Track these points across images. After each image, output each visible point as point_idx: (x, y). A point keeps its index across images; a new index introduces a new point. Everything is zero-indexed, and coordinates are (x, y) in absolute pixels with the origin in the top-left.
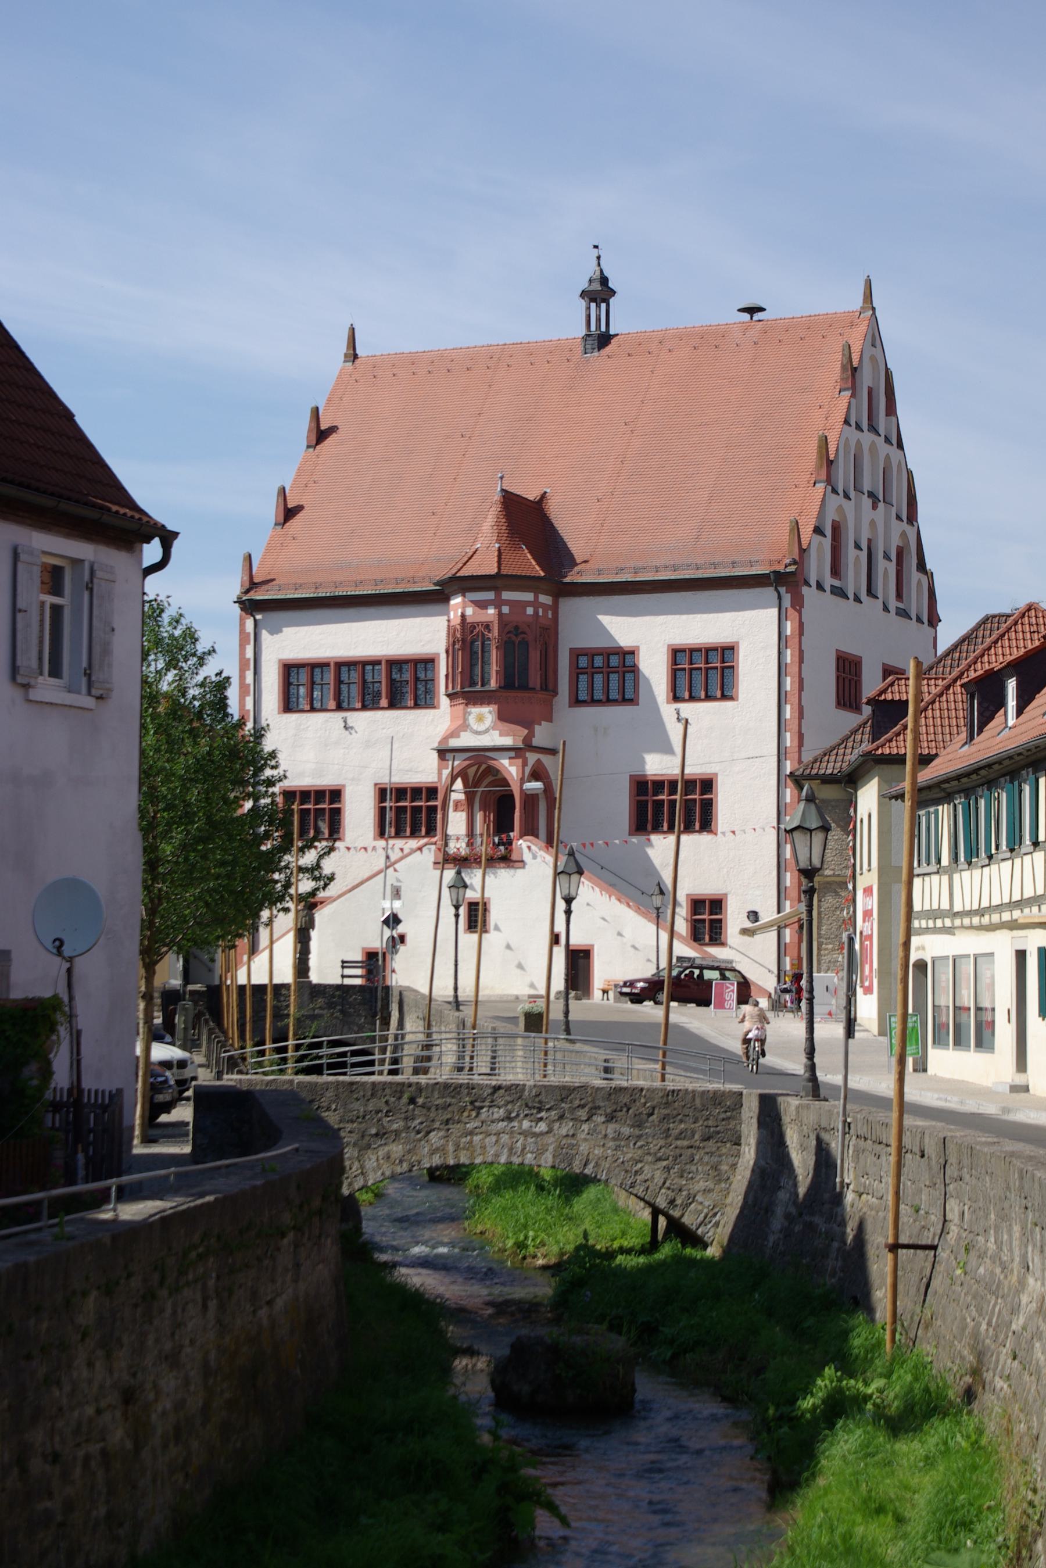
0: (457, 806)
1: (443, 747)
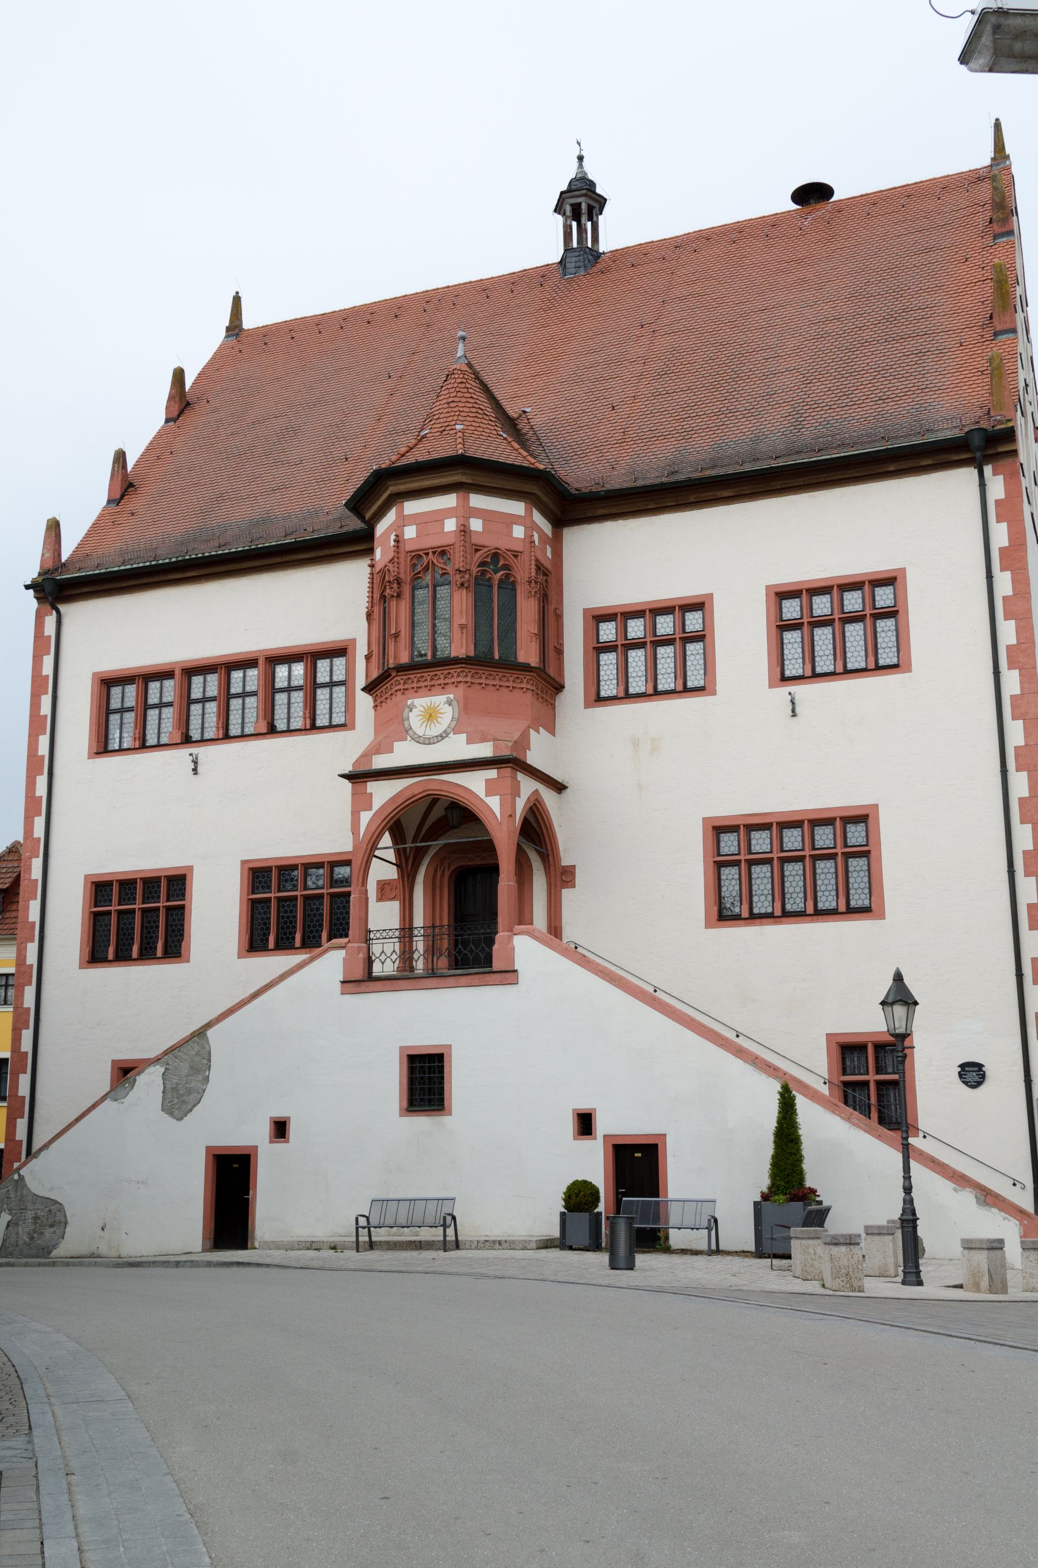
0: (385, 890)
1: (363, 768)
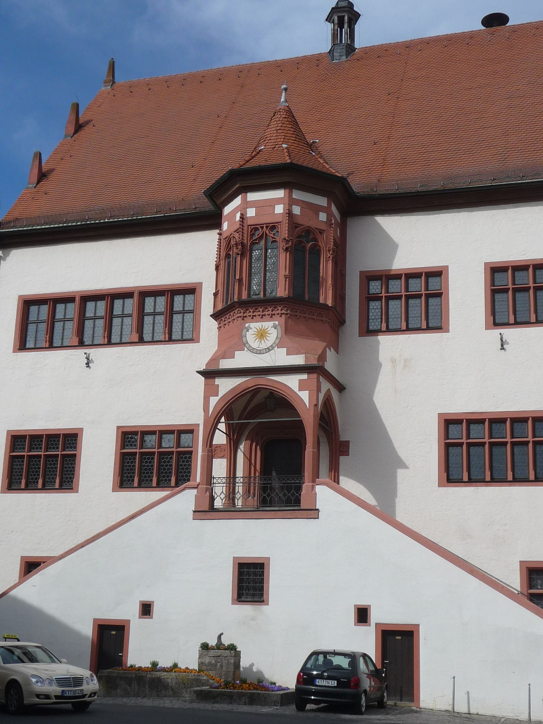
1: (213, 368)
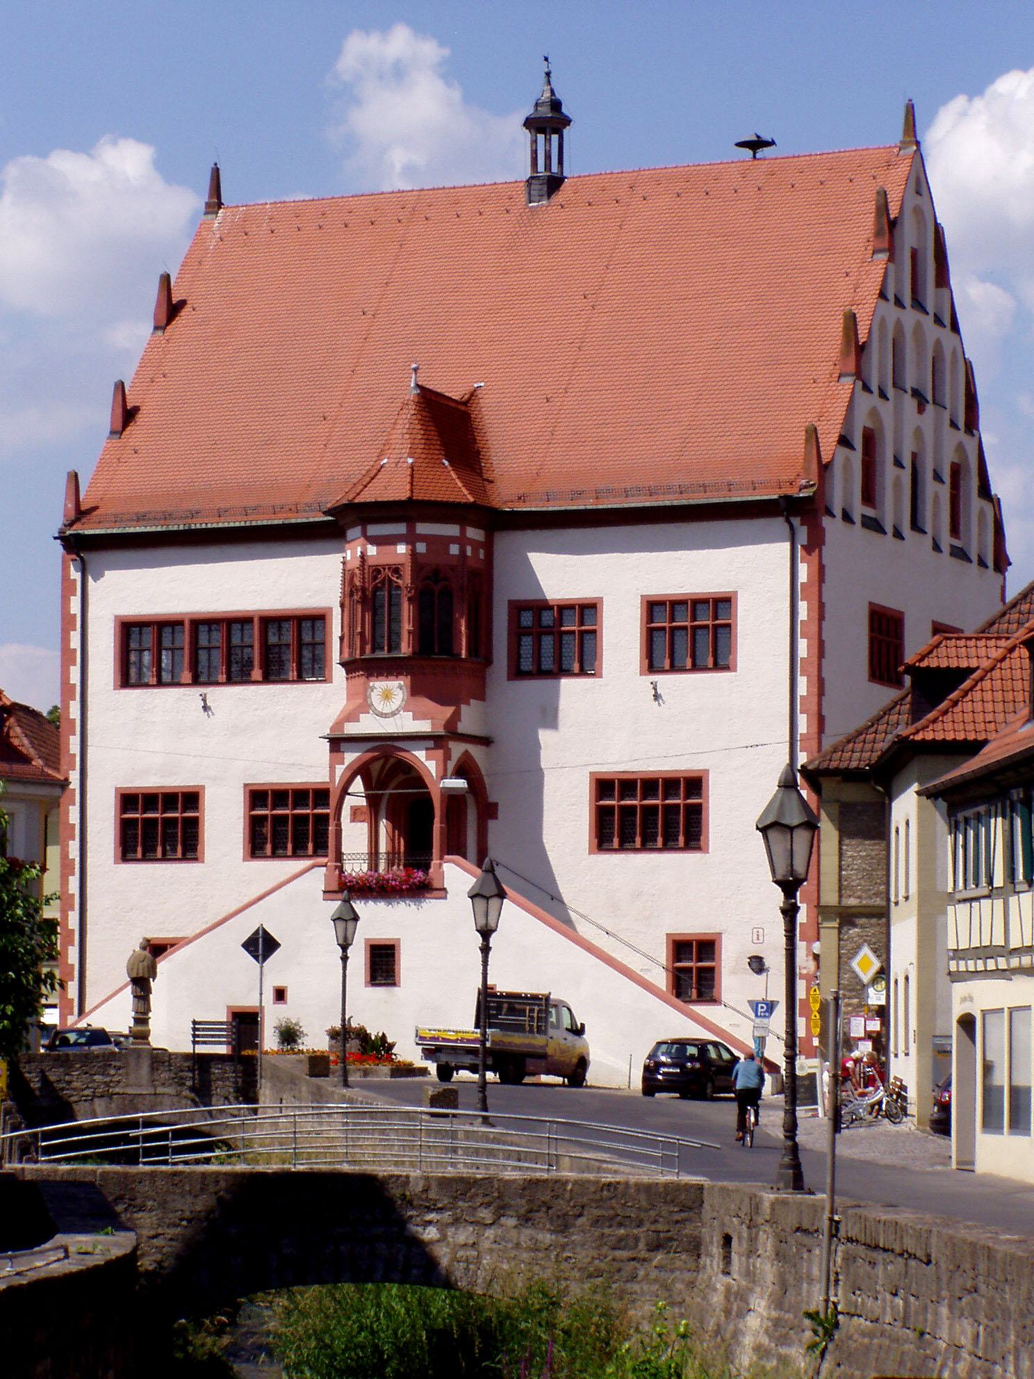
0: (356, 813)
1: (338, 734)
